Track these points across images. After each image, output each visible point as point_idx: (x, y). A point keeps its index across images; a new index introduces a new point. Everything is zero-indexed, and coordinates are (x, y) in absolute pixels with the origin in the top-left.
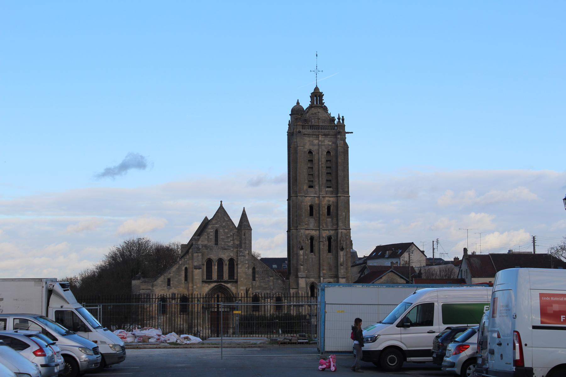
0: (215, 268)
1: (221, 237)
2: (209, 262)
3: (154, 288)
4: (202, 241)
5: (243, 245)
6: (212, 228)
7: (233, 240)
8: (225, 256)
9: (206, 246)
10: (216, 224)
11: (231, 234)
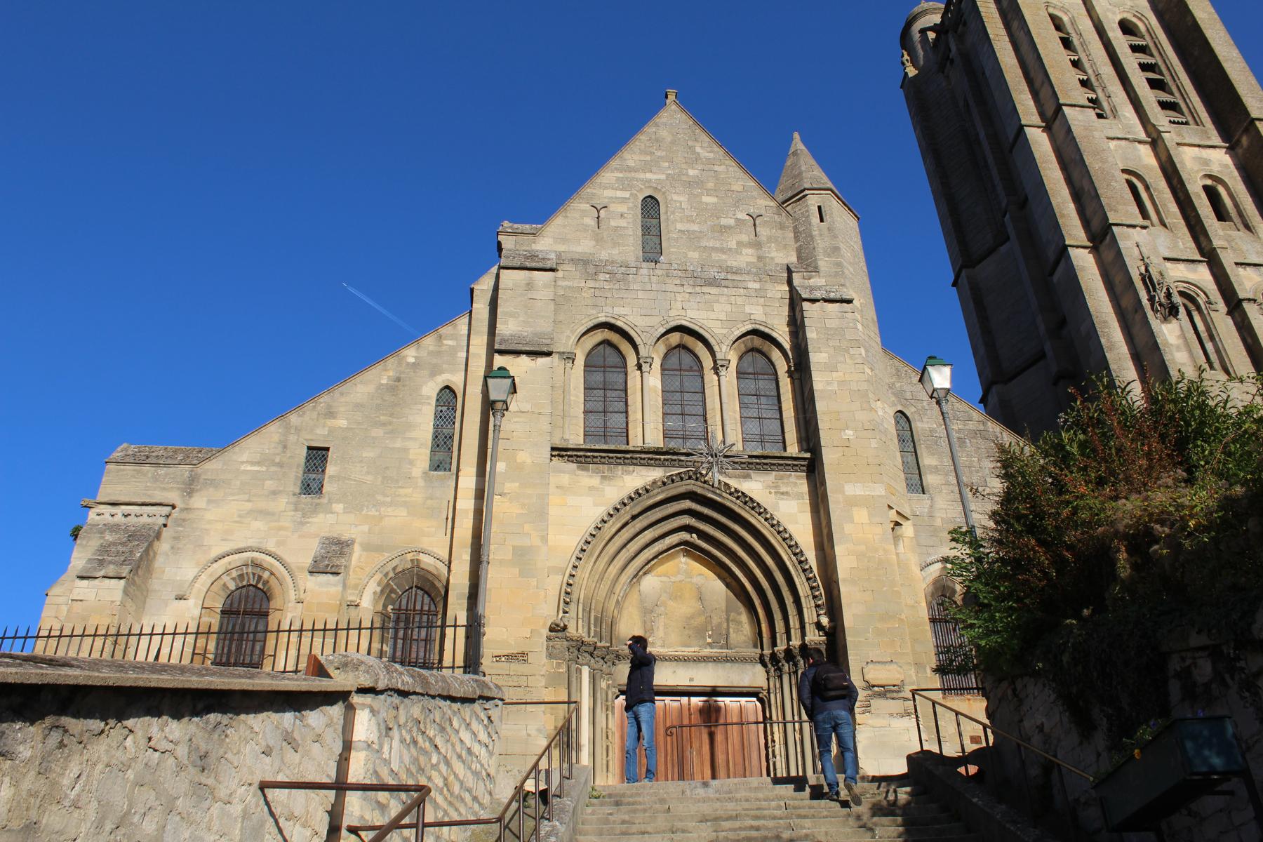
0: (647, 388)
1: (674, 223)
2: (610, 348)
3: (198, 501)
4: (564, 240)
5: (823, 263)
6: (624, 184)
7: (758, 245)
8: (721, 319)
9: (586, 264)
10: (647, 167)
11: (742, 216)
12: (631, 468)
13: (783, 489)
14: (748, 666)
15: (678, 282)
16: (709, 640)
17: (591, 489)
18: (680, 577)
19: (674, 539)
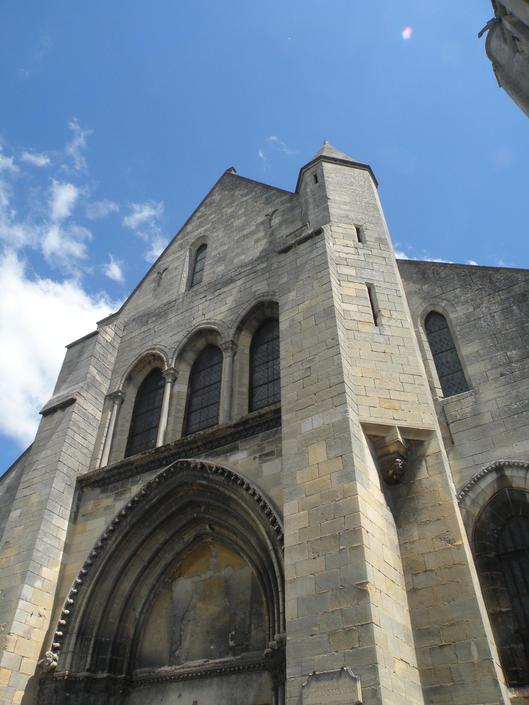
12: (138, 477)
13: (267, 450)
14: (254, 676)
15: (203, 295)
16: (232, 643)
17: (107, 508)
18: (209, 573)
19: (188, 537)
